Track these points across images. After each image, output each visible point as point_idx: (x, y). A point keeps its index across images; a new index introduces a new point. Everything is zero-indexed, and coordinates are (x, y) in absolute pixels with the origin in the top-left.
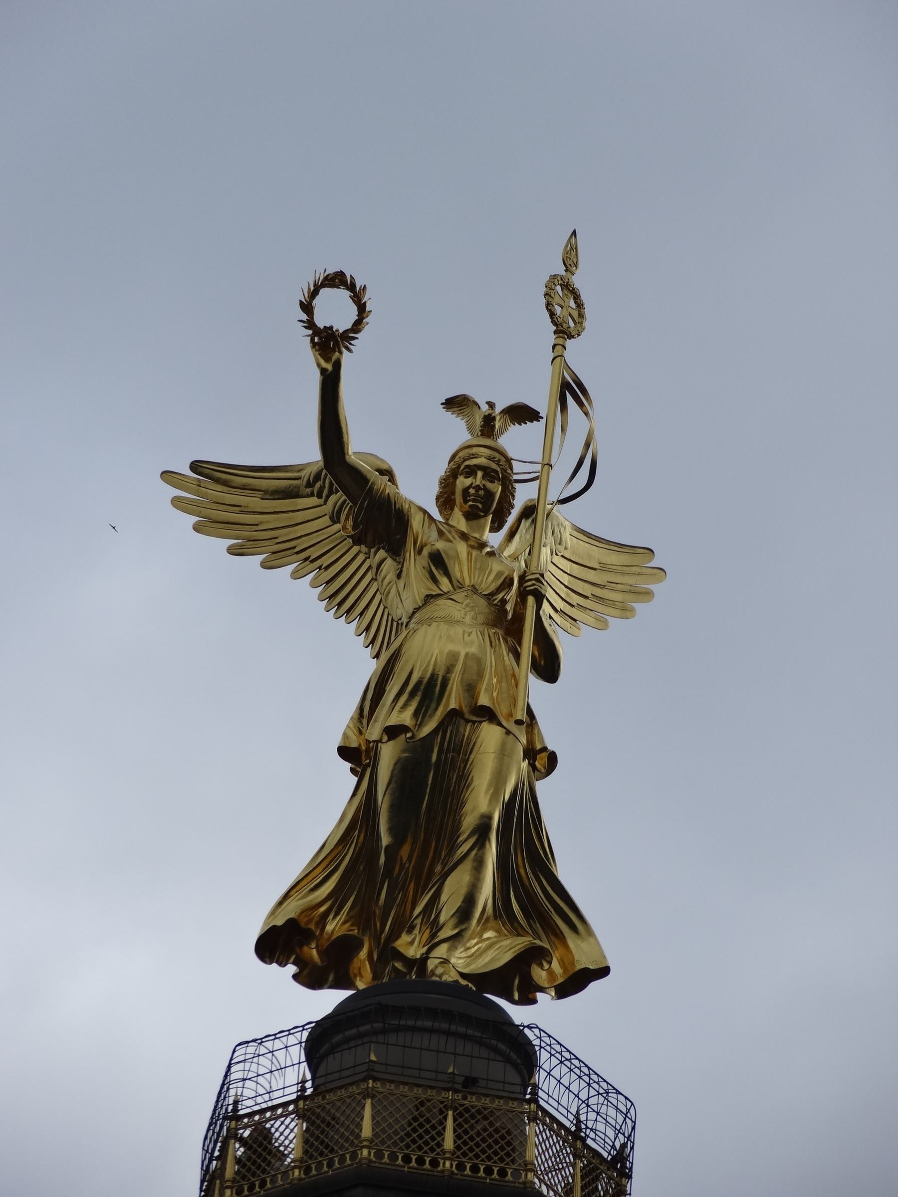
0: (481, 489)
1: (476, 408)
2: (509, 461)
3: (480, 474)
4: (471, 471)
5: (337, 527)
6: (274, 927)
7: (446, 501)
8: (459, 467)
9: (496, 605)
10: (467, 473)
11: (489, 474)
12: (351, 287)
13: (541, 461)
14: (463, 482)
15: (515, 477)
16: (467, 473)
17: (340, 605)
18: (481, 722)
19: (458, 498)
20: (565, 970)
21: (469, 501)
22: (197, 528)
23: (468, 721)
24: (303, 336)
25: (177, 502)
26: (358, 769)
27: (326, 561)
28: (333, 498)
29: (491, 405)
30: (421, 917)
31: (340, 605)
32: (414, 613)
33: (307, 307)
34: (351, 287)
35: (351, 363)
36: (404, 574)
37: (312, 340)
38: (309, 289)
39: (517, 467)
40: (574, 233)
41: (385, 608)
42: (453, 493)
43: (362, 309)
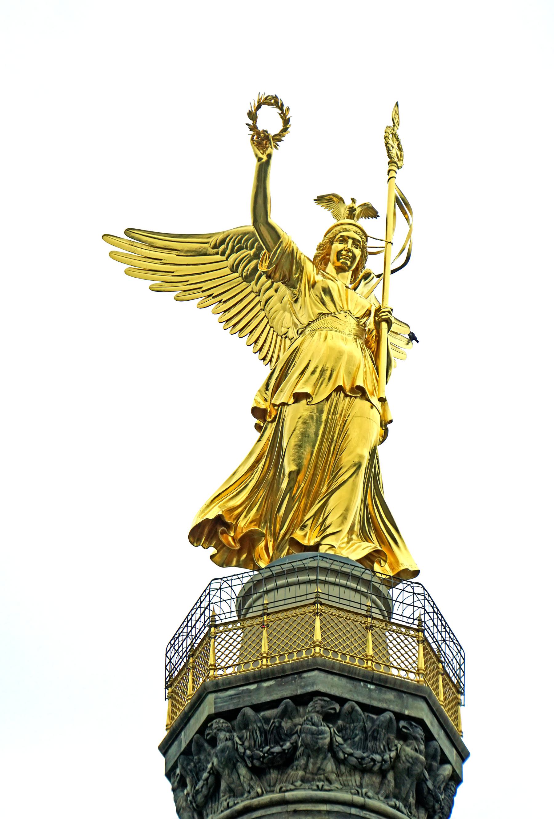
0: (350, 252)
1: (342, 202)
2: (366, 236)
3: (350, 241)
4: (343, 240)
5: (236, 275)
6: (207, 520)
8: (336, 236)
9: (361, 325)
10: (340, 241)
12: (281, 108)
13: (384, 239)
14: (337, 246)
16: (340, 241)
17: (234, 326)
18: (356, 397)
19: (333, 257)
21: (342, 259)
22: (127, 272)
23: (346, 395)
24: (248, 133)
25: (112, 255)
26: (262, 425)
27: (225, 297)
28: (234, 256)
29: (353, 200)
30: (311, 520)
31: (234, 326)
32: (309, 324)
33: (252, 115)
34: (281, 108)
35: (279, 156)
36: (300, 300)
37: (252, 139)
38: (255, 104)
39: (371, 243)
40: (397, 104)
41: (271, 327)
42: (329, 254)
43: (286, 122)
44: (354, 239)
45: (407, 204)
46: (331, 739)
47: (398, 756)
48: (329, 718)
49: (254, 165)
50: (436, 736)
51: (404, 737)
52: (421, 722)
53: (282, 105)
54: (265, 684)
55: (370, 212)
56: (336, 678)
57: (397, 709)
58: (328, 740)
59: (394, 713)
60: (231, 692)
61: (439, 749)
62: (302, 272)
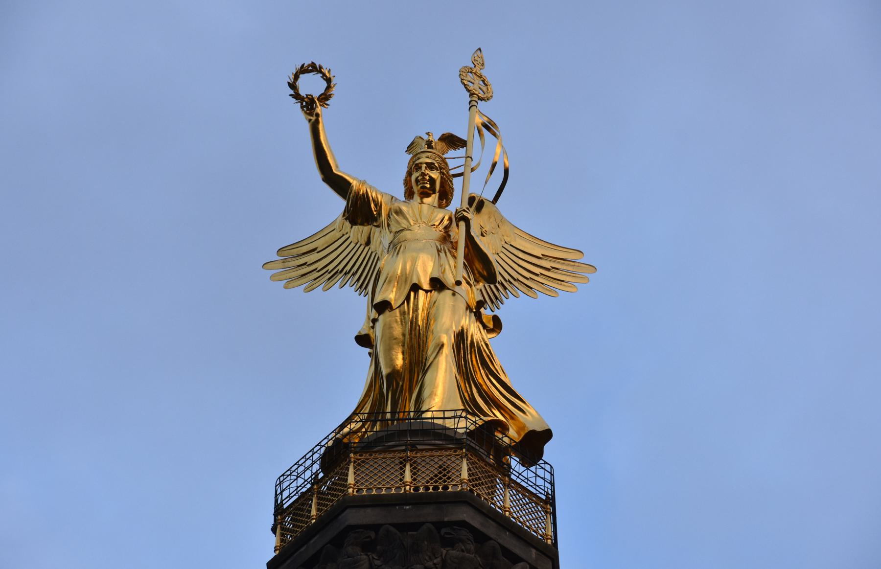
7: (409, 194)
11: (430, 166)
15: (451, 172)
20: (518, 433)
33: (293, 86)
34: (321, 72)
37: (302, 107)
43: (329, 81)
44: (426, 163)
45: (494, 125)
46: (371, 565)
47: (444, 561)
48: (367, 547)
49: (307, 128)
50: (493, 536)
51: (450, 543)
52: (464, 524)
53: (321, 67)
54: (312, 541)
55: (452, 141)
56: (369, 510)
59: (433, 523)
60: (289, 561)
61: (498, 546)
62: (381, 207)
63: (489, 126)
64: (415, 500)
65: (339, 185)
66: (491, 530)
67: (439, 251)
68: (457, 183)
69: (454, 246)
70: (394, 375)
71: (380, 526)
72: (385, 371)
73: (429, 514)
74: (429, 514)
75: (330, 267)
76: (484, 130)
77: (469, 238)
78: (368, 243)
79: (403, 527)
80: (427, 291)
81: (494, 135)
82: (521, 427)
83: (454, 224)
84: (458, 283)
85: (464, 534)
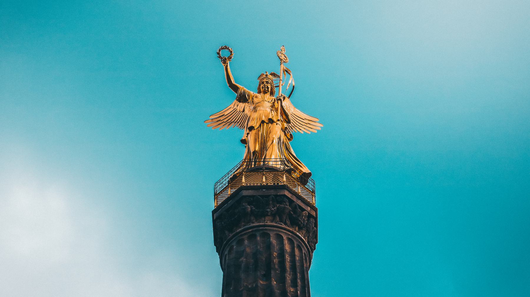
33: (218, 54)
43: (231, 52)
51: (280, 202)
56: (250, 191)
57: (274, 194)
58: (250, 209)
63: (287, 71)
64: (267, 187)
65: (235, 88)
66: (294, 199)
67: (271, 110)
68: (276, 89)
69: (277, 110)
70: (254, 152)
71: (254, 196)
72: (252, 150)
73: (272, 192)
74: (272, 192)
75: (229, 121)
76: (286, 72)
77: (282, 106)
78: (244, 111)
79: (262, 196)
80: (267, 123)
81: (289, 74)
82: (301, 171)
83: (276, 102)
84: (278, 120)
85: (285, 199)
